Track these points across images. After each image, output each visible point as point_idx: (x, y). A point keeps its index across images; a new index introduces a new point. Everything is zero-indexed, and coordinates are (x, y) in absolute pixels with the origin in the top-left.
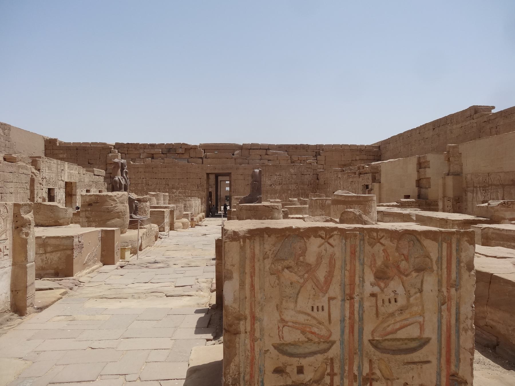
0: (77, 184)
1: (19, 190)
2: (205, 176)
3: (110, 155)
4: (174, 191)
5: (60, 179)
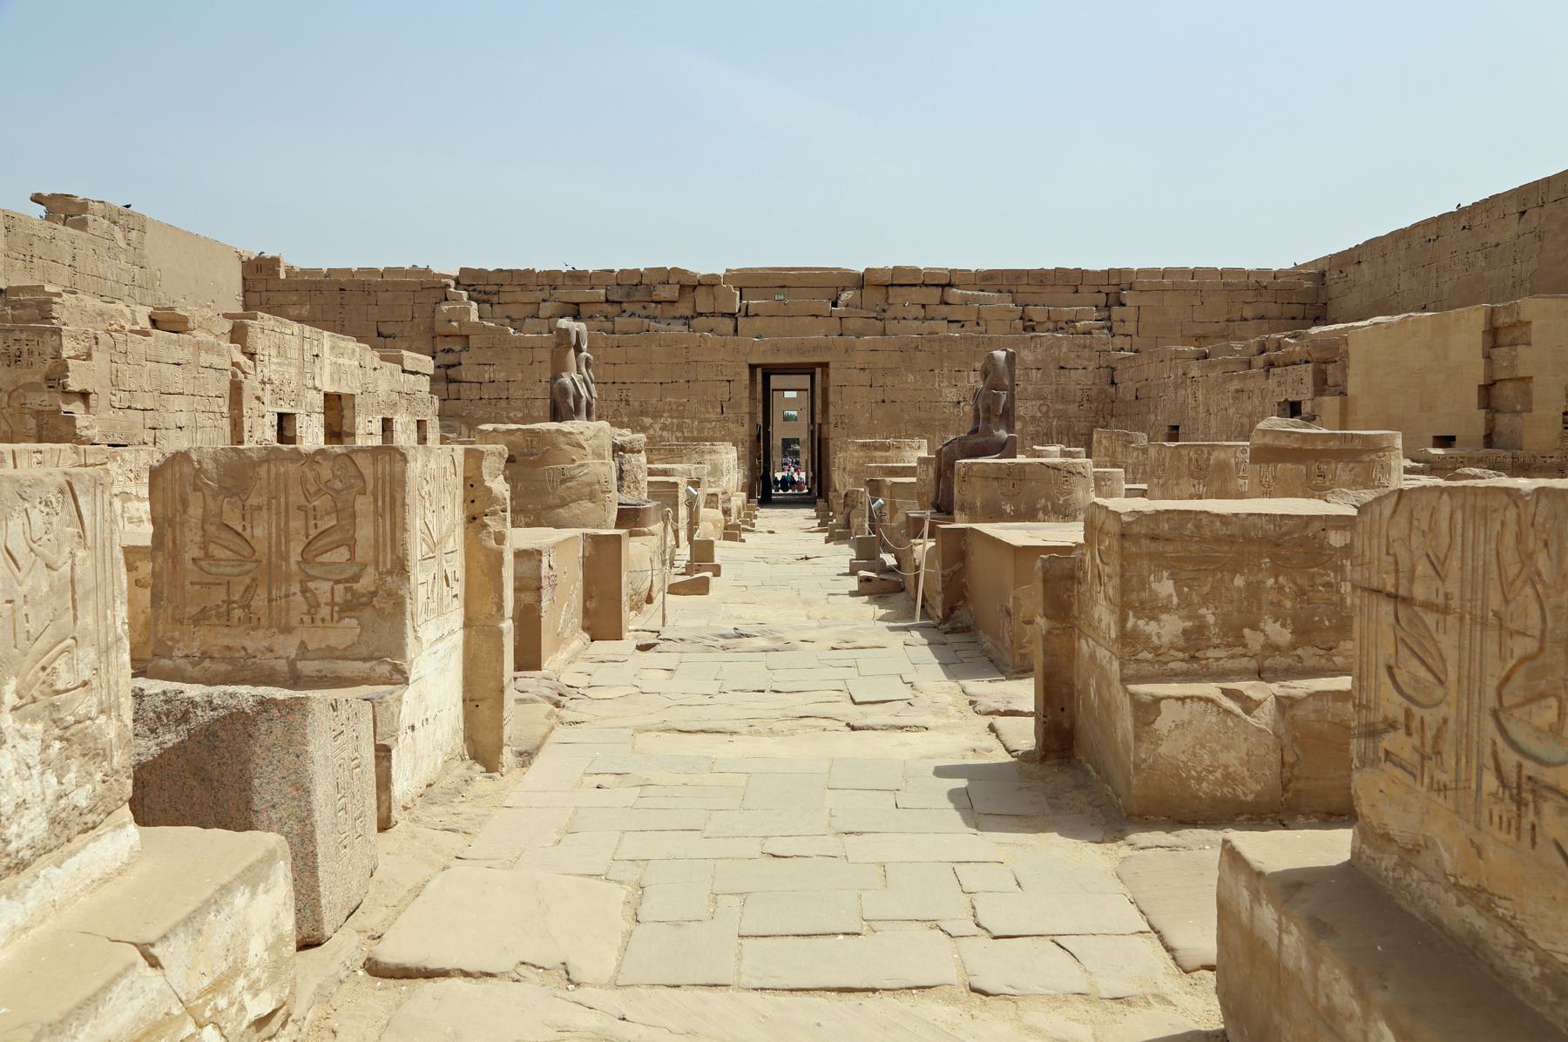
0: (358, 400)
1: (201, 418)
2: (747, 370)
3: (445, 307)
4: (648, 421)
5: (310, 383)
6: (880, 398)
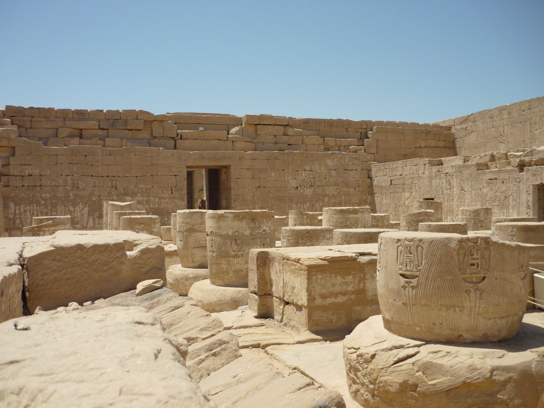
6: (258, 185)
